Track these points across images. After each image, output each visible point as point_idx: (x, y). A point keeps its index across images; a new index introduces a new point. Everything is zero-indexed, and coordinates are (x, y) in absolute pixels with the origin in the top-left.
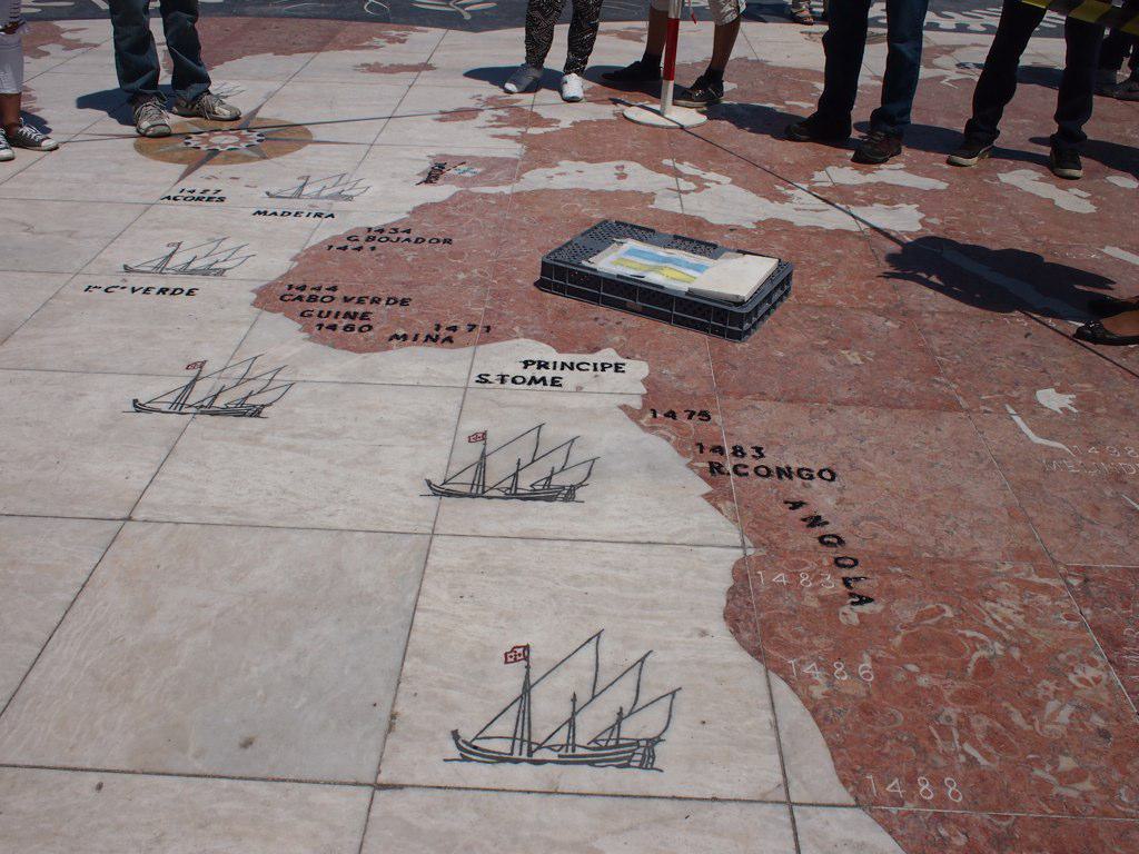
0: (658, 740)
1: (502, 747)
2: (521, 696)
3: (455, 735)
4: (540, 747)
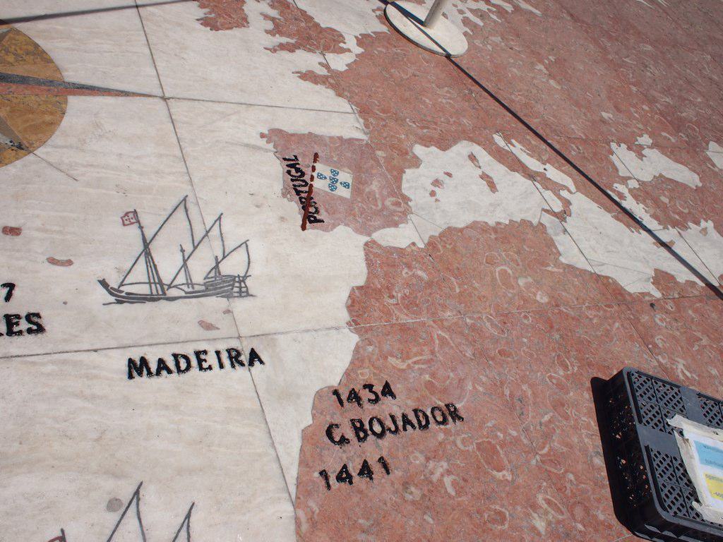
0: (246, 277)
1: (144, 290)
3: (103, 283)
4: (170, 286)
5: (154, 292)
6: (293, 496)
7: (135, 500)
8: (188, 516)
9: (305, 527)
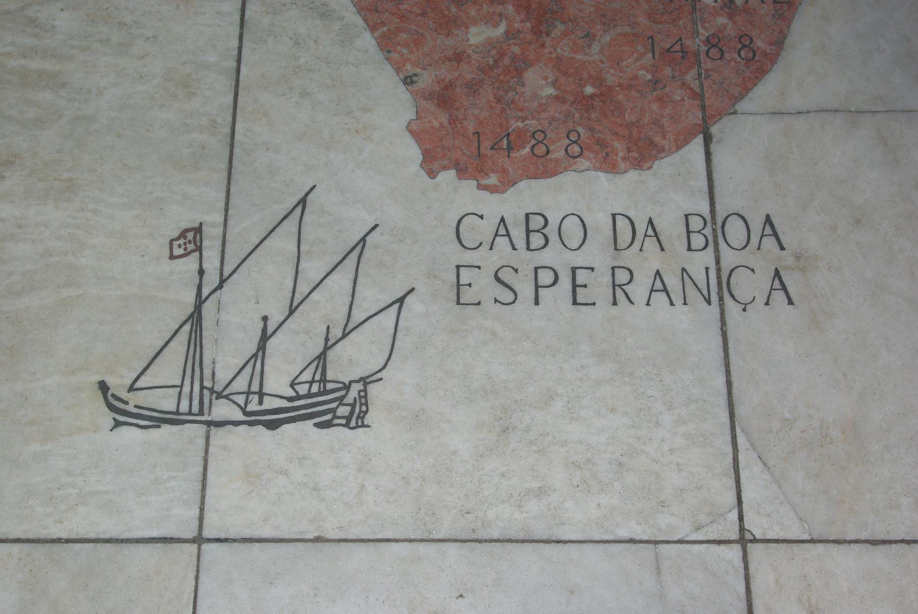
2: (192, 316)
5: (184, 407)
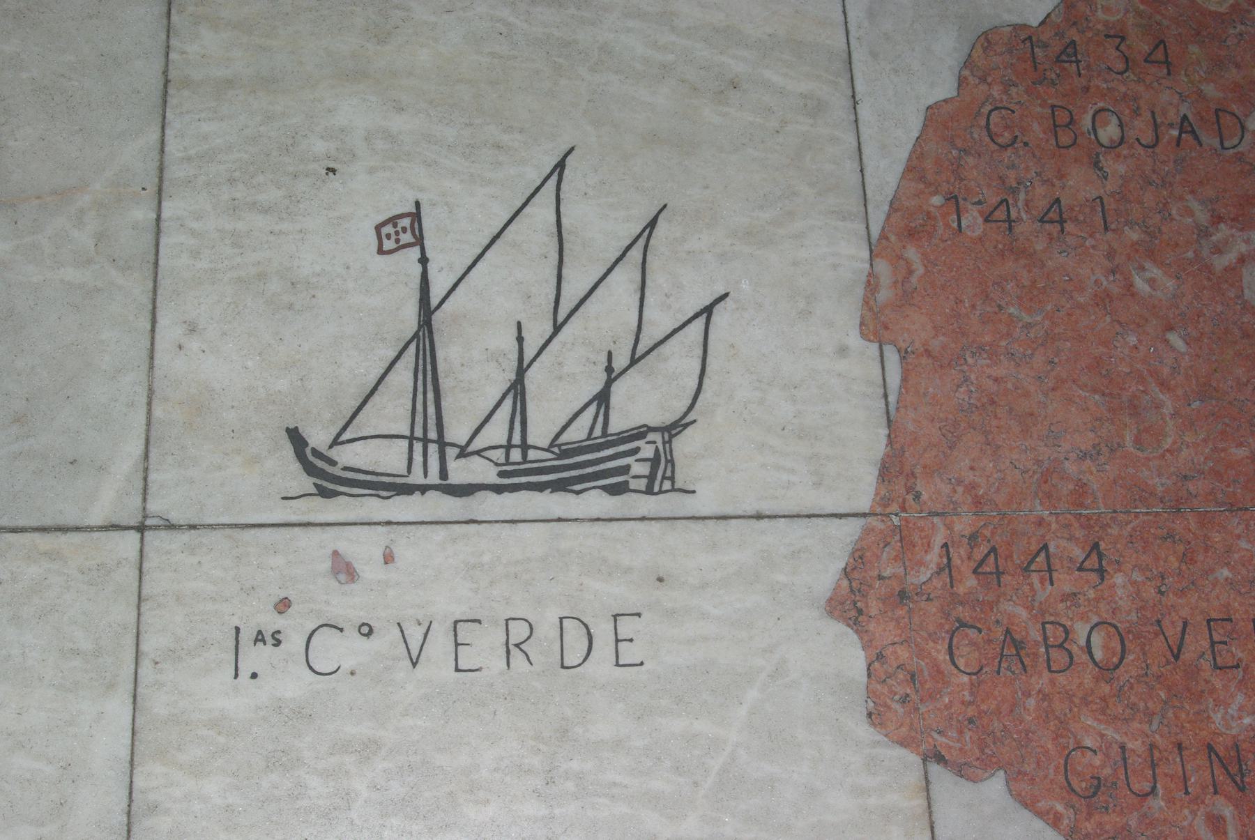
6: (875, 231)
7: (555, 177)
8: (652, 224)
9: (884, 295)
